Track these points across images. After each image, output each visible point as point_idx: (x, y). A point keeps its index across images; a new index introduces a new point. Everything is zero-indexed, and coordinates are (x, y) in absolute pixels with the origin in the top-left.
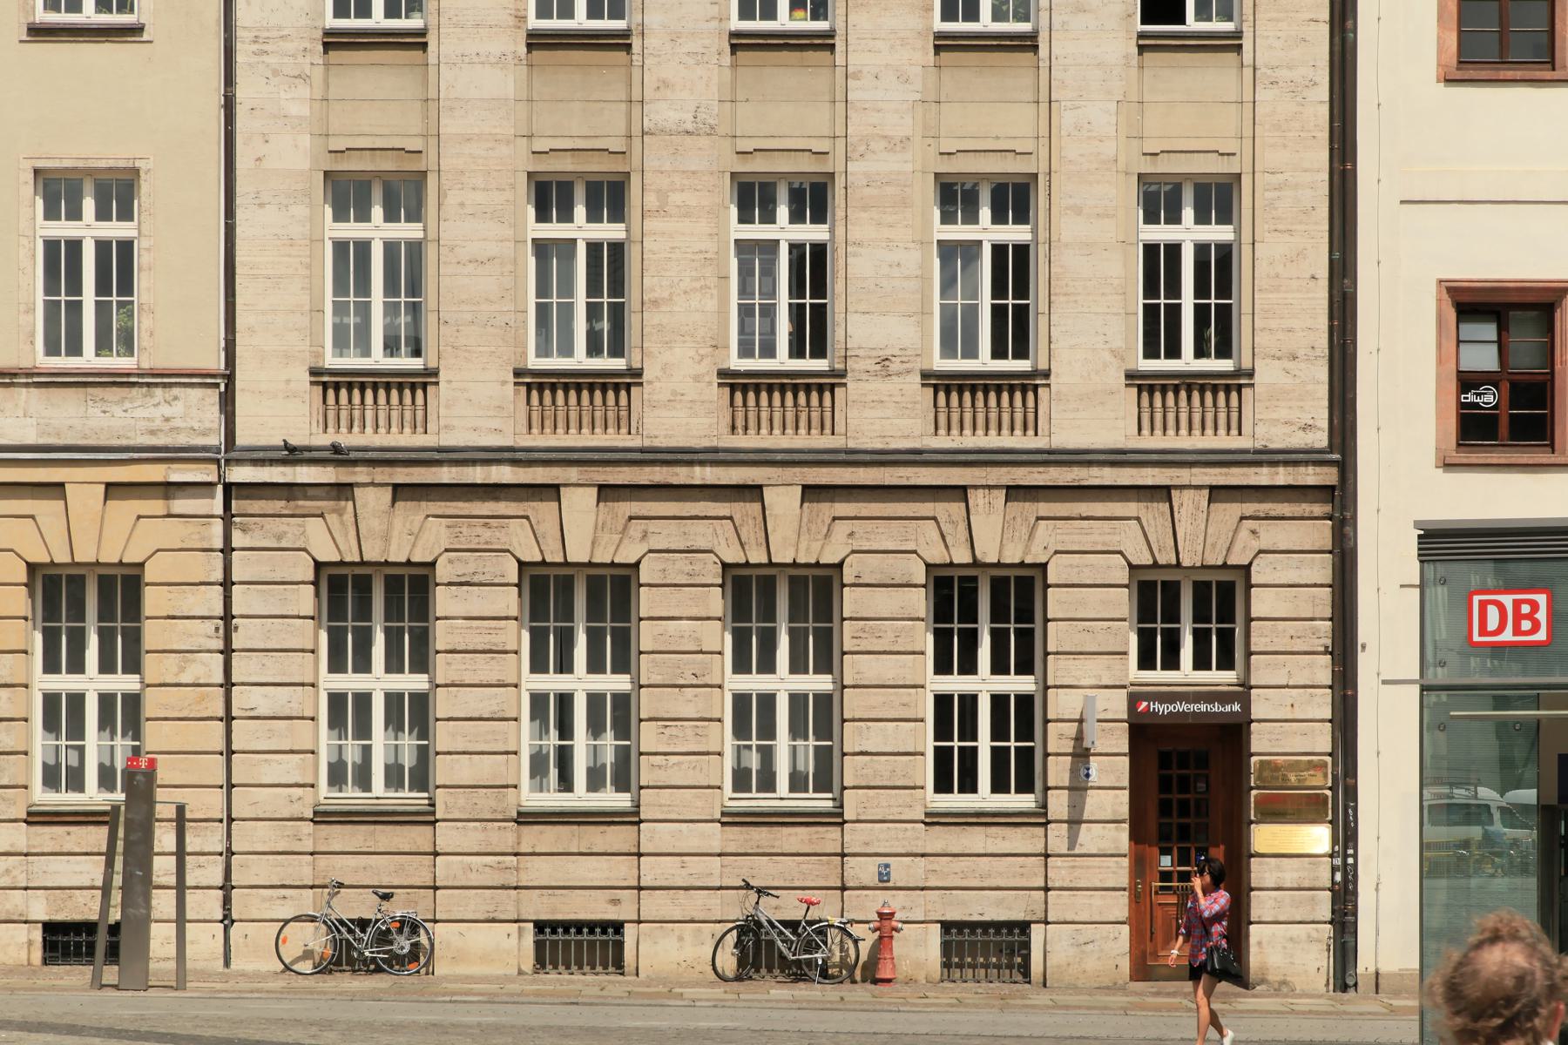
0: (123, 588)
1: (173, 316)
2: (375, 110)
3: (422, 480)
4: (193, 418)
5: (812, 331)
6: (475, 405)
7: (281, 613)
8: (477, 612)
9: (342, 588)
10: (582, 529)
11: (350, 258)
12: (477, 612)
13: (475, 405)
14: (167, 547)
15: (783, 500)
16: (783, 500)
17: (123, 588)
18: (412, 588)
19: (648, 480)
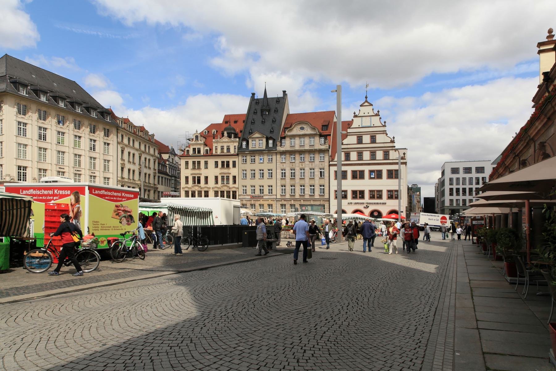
0: (272, 205)
1: (274, 193)
2: (283, 182)
3: (285, 200)
4: (275, 197)
5: (304, 193)
6: (288, 196)
7: (279, 206)
8: (288, 206)
9: (282, 205)
10: (293, 202)
11: (282, 189)
12: (288, 206)
13: (288, 196)
14: (274, 203)
15: (302, 201)
16: (302, 201)
17: (272, 205)
18: (285, 205)
19: (295, 200)
